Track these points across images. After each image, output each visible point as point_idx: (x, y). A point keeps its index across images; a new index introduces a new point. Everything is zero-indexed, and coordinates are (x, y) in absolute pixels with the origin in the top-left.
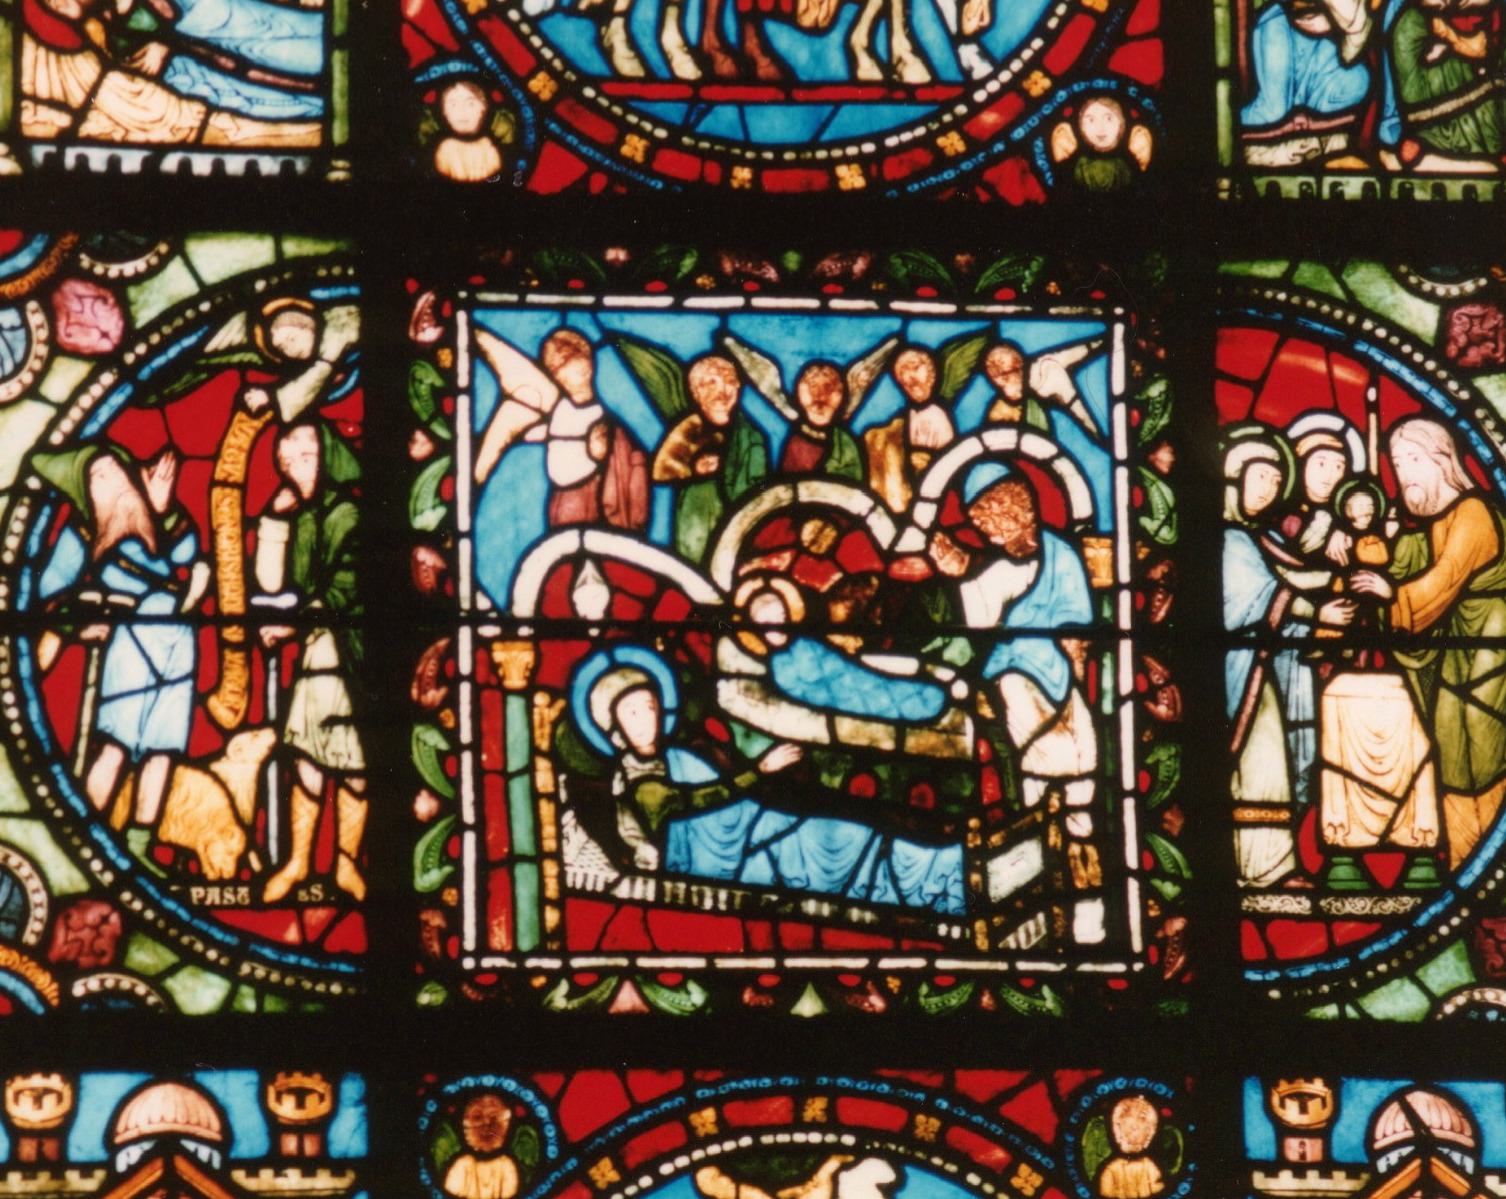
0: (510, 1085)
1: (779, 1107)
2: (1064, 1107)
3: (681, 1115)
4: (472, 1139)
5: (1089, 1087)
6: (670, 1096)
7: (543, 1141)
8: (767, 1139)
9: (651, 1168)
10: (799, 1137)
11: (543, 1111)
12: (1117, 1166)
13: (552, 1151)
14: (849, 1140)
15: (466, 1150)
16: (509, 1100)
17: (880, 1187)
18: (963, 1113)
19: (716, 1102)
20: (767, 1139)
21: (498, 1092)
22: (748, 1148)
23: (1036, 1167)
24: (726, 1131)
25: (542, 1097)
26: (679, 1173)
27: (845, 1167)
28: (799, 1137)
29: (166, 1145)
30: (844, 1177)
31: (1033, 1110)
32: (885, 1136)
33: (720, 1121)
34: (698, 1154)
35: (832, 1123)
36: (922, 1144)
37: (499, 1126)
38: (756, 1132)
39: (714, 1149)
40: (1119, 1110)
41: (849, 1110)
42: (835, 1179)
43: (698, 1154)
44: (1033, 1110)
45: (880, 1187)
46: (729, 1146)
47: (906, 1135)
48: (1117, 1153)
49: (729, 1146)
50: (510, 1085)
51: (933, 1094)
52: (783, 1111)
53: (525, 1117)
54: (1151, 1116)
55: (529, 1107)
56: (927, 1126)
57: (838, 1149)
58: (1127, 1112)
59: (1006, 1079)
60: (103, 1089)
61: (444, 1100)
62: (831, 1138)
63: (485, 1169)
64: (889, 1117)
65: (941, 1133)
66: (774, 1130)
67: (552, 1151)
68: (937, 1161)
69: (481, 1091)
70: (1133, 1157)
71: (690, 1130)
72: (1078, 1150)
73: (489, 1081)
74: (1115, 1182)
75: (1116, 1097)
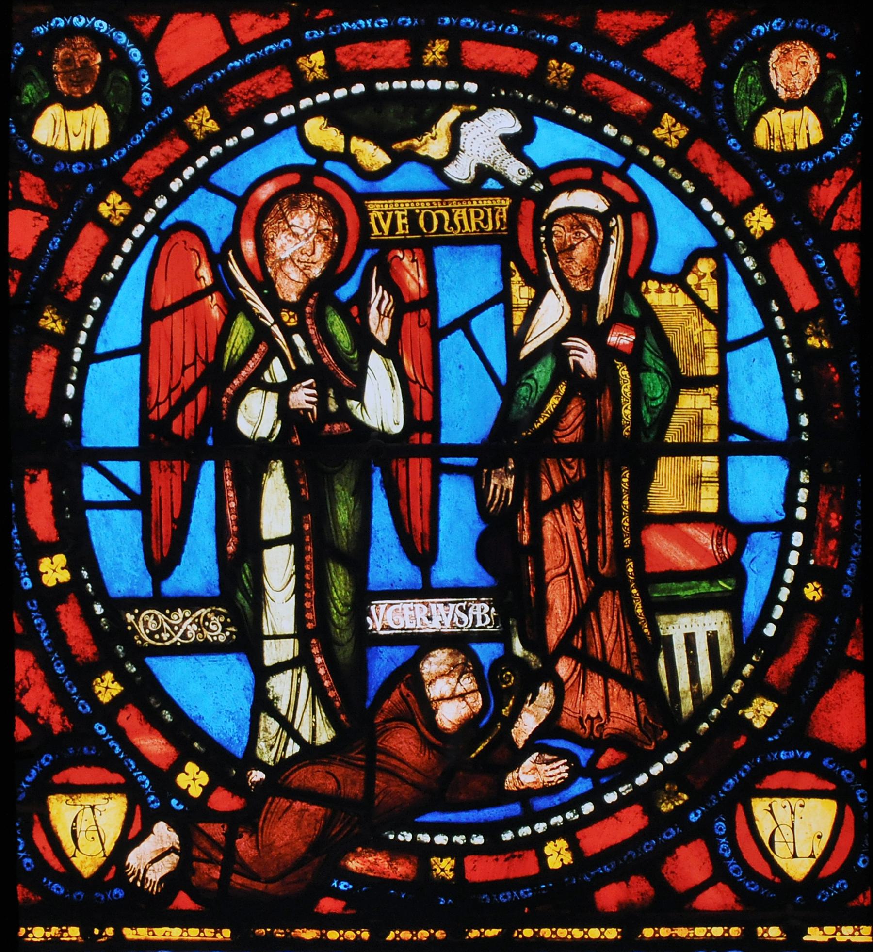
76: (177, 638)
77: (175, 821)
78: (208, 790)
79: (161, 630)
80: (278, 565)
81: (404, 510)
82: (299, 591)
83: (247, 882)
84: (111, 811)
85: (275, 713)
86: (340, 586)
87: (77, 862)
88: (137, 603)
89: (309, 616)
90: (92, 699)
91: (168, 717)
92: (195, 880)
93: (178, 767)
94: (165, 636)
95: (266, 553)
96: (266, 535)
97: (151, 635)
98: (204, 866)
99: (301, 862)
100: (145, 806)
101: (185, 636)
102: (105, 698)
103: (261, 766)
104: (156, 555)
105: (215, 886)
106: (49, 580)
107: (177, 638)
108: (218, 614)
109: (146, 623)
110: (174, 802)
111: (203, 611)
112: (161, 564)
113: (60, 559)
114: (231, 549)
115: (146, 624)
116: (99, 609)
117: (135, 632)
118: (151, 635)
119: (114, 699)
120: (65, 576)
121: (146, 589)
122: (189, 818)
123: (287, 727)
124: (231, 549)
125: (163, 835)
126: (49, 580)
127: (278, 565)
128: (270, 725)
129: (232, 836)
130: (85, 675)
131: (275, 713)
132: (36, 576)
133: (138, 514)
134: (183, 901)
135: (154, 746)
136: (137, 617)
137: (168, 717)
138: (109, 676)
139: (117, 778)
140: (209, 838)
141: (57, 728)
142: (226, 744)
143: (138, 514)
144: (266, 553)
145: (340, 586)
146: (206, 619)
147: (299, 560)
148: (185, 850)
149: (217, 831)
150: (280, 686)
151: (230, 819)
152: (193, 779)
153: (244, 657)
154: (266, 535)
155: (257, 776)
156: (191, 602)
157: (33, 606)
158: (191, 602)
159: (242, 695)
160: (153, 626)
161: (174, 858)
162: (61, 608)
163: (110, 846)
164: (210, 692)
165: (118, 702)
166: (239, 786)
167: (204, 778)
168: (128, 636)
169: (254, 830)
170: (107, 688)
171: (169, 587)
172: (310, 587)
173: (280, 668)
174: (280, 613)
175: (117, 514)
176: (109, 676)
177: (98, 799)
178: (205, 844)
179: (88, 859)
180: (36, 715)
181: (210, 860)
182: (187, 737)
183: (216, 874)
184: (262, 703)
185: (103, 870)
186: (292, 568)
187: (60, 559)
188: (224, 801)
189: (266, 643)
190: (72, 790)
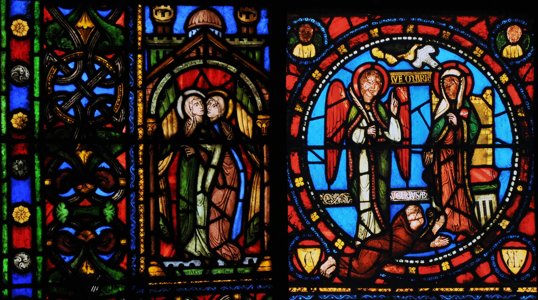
0: (313, 21)
1: (398, 28)
2: (490, 28)
3: (367, 31)
4: (301, 38)
5: (499, 22)
6: (363, 24)
7: (323, 39)
8: (395, 39)
9: (357, 48)
10: (405, 38)
11: (323, 29)
12: (508, 47)
13: (326, 42)
14: (420, 39)
15: (300, 42)
16: (313, 26)
17: (430, 54)
18: (458, 30)
19: (379, 27)
20: (395, 39)
21: (310, 23)
22: (388, 41)
23: (481, 48)
24: (382, 35)
25: (323, 25)
26: (366, 50)
27: (419, 48)
28: (405, 38)
29: (204, 29)
30: (419, 51)
31: (481, 28)
32: (432, 37)
33: (380, 32)
34: (372, 44)
35: (416, 33)
36: (444, 40)
37: (310, 34)
38: (391, 36)
39: (377, 42)
40: (509, 29)
41: (422, 29)
42: (416, 51)
43: (372, 44)
44: (481, 28)
45: (430, 54)
46: (382, 41)
47: (439, 37)
48: (508, 43)
49: (382, 41)
50: (313, 21)
51: (448, 24)
52: (400, 29)
53: (318, 31)
54: (520, 31)
55: (319, 28)
56: (446, 34)
57: (417, 42)
58: (512, 29)
59: (472, 19)
60: (184, 11)
61: (293, 26)
62: (415, 38)
63: (305, 48)
64: (433, 31)
65: (451, 36)
66: (397, 35)
67: (326, 42)
68: (449, 46)
69: (304, 22)
70: (514, 44)
71: (370, 35)
72: (495, 42)
73: (307, 20)
74: (507, 52)
75: (508, 25)
76: (335, 202)
77: (334, 256)
78: (344, 247)
79: (330, 200)
80: (364, 181)
81: (401, 164)
82: (370, 188)
83: (355, 274)
84: (316, 253)
85: (363, 224)
86: (382, 187)
87: (306, 268)
88: (324, 192)
89: (373, 196)
90: (310, 220)
91: (332, 226)
92: (340, 274)
93: (335, 240)
94: (332, 201)
95: (361, 177)
96: (361, 172)
97: (327, 201)
98: (343, 270)
99: (371, 268)
100: (326, 252)
101: (337, 202)
102: (314, 220)
103: (359, 240)
104: (329, 178)
105: (346, 275)
106: (298, 185)
107: (335, 202)
108: (347, 195)
109: (326, 198)
110: (334, 251)
111: (343, 194)
112: (330, 180)
113: (301, 179)
114: (351, 176)
115: (326, 198)
116: (312, 194)
117: (323, 200)
118: (327, 201)
119: (317, 220)
120: (302, 184)
121: (326, 188)
122: (339, 255)
123: (367, 228)
124: (351, 176)
125: (331, 260)
126: (298, 185)
127: (364, 181)
128: (362, 228)
129: (351, 261)
130: (308, 213)
131: (363, 224)
132: (294, 184)
133: (324, 165)
134: (337, 280)
135: (328, 234)
136: (323, 196)
137: (332, 226)
138: (315, 213)
139: (317, 244)
140: (344, 261)
141: (300, 229)
142: (349, 234)
143: (324, 165)
144: (361, 177)
145: (382, 187)
146: (343, 196)
147: (370, 179)
148: (337, 265)
149: (347, 259)
150: (365, 216)
151: (350, 256)
152: (340, 244)
153: (354, 208)
154: (361, 172)
155: (358, 243)
156: (339, 191)
157: (293, 192)
158: (339, 191)
159: (354, 219)
160: (328, 199)
161: (334, 267)
162: (301, 193)
163: (315, 264)
164: (344, 218)
165: (318, 221)
166: (353, 246)
167: (343, 244)
168: (320, 201)
169: (357, 259)
170: (315, 217)
171: (333, 187)
172: (374, 187)
173: (365, 211)
174: (365, 195)
175: (317, 165)
176: (315, 213)
177: (312, 250)
178: (343, 263)
179: (309, 268)
180: (294, 225)
181: (345, 268)
182: (338, 231)
183: (346, 272)
184: (360, 221)
185: (313, 271)
186: (368, 181)
187: (301, 179)
188: (348, 250)
189: (361, 203)
190: (304, 247)
